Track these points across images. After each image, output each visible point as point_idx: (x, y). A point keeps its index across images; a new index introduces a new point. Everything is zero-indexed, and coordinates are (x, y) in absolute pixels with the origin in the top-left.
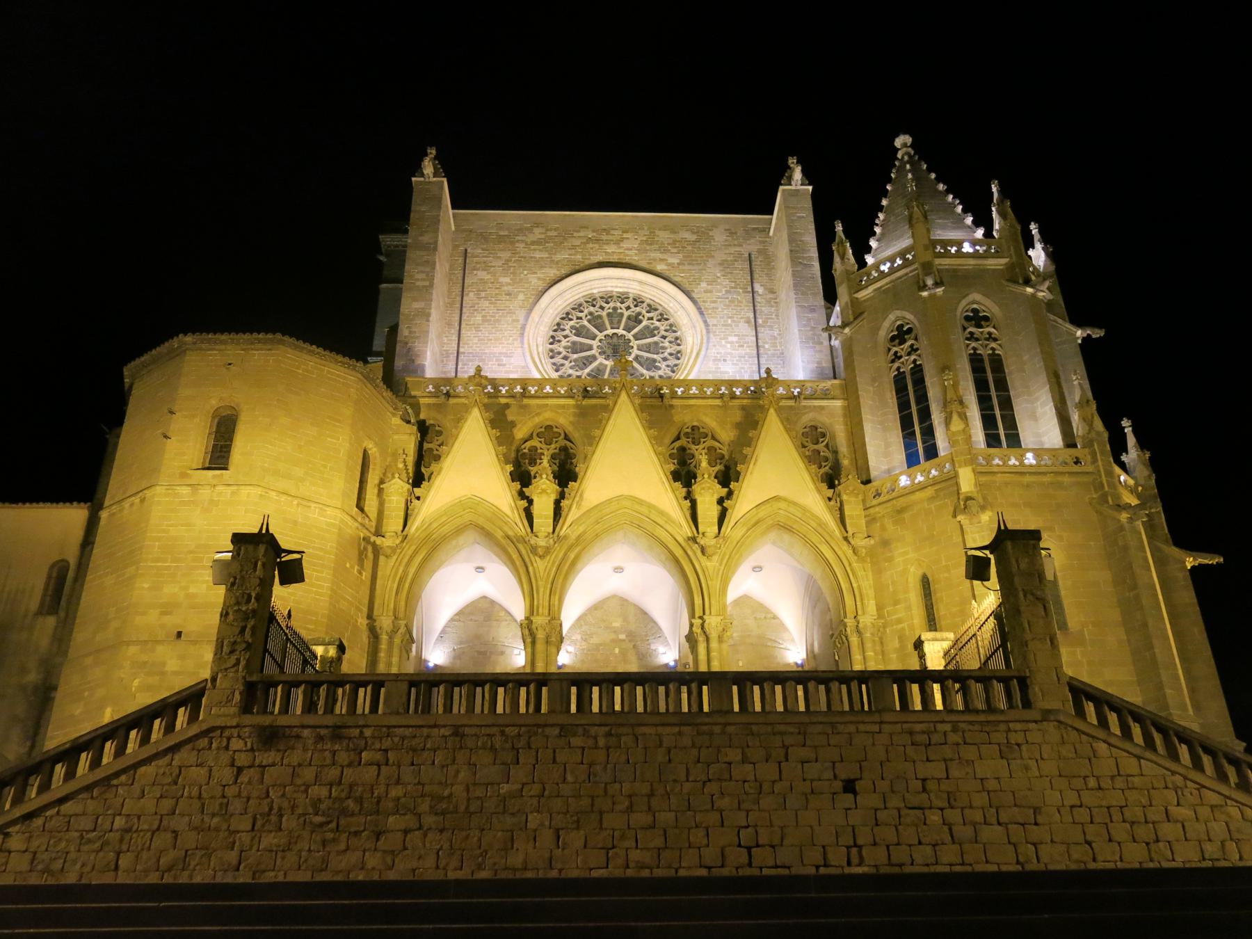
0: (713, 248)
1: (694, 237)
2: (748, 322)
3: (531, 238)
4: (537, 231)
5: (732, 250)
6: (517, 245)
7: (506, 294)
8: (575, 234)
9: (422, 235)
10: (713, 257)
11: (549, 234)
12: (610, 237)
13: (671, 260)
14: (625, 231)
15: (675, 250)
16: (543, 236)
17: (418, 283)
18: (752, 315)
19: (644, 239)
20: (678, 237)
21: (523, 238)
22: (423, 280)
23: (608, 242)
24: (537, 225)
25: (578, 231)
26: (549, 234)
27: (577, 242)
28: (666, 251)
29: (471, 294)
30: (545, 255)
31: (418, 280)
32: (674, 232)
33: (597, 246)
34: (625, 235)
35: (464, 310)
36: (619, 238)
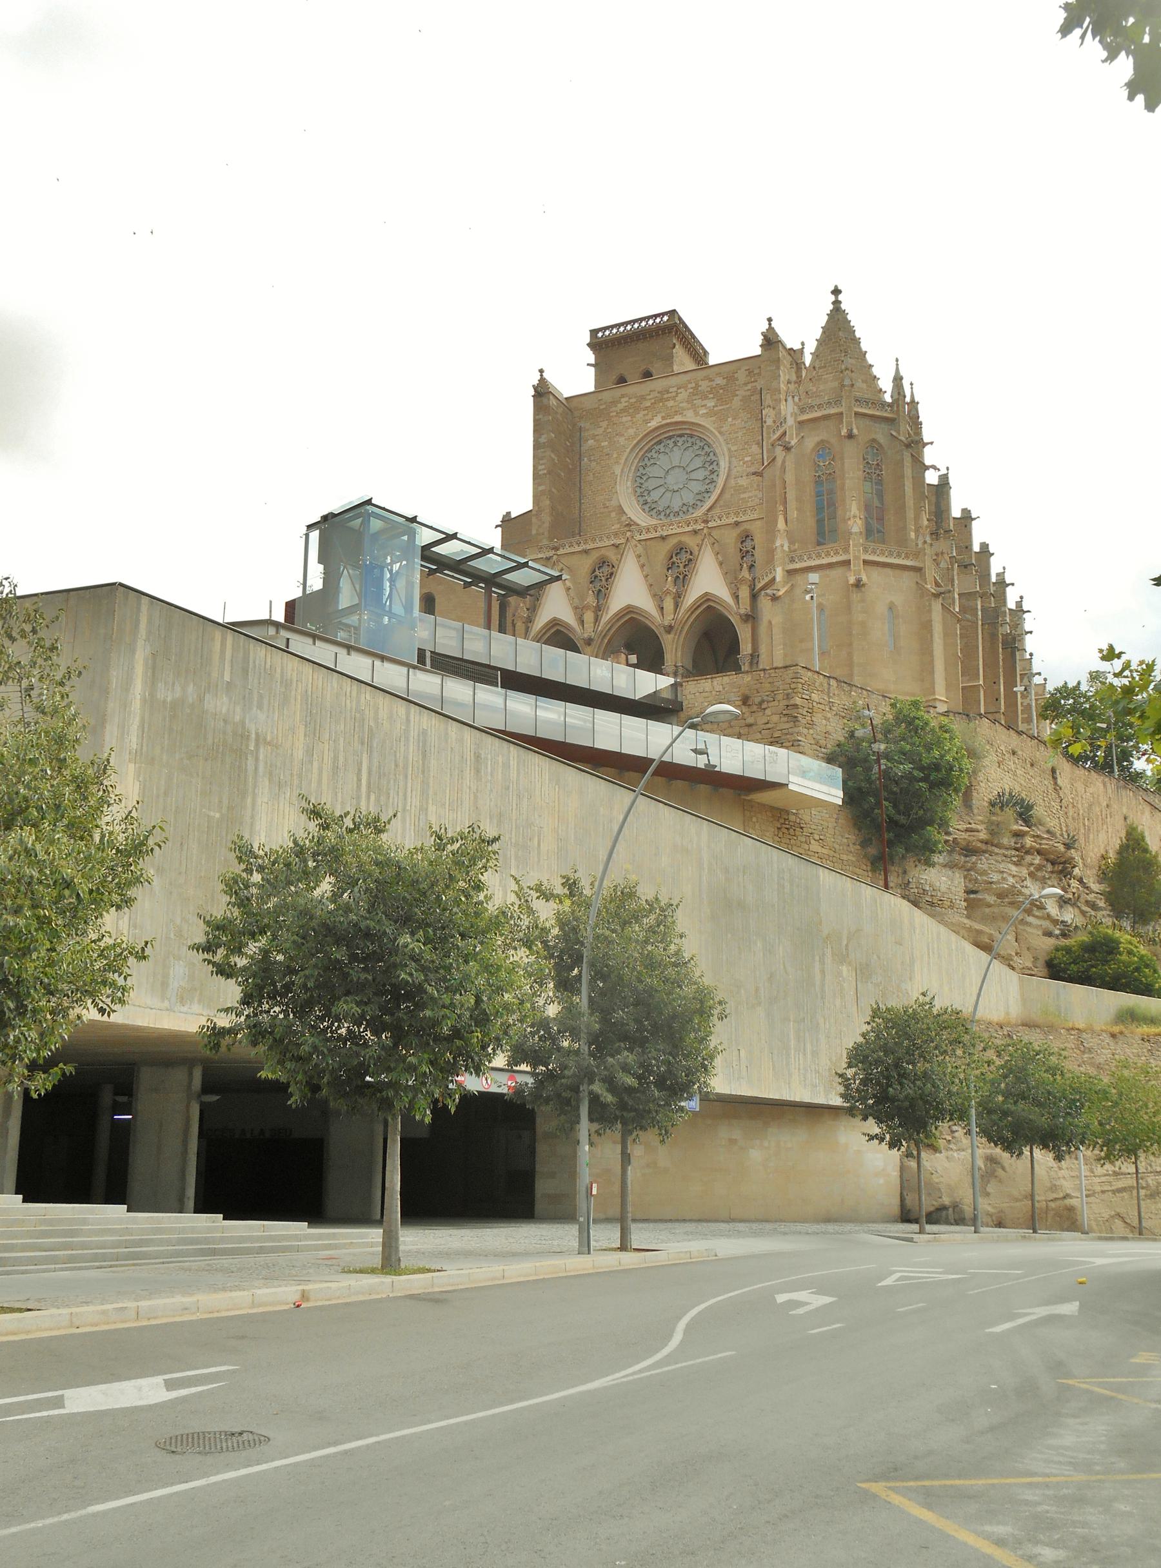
0: (737, 388)
2: (758, 444)
3: (620, 406)
5: (749, 387)
6: (611, 414)
7: (608, 454)
8: (648, 397)
9: (540, 437)
10: (737, 395)
11: (631, 401)
12: (669, 395)
13: (708, 405)
14: (680, 388)
15: (712, 396)
16: (627, 404)
17: (540, 473)
18: (761, 438)
19: (692, 390)
20: (714, 384)
21: (614, 409)
22: (543, 469)
23: (668, 400)
24: (623, 396)
25: (650, 394)
26: (631, 401)
27: (648, 404)
28: (706, 398)
29: (586, 459)
30: (629, 418)
31: (540, 470)
32: (711, 380)
33: (661, 404)
34: (679, 391)
35: (582, 472)
36: (674, 394)
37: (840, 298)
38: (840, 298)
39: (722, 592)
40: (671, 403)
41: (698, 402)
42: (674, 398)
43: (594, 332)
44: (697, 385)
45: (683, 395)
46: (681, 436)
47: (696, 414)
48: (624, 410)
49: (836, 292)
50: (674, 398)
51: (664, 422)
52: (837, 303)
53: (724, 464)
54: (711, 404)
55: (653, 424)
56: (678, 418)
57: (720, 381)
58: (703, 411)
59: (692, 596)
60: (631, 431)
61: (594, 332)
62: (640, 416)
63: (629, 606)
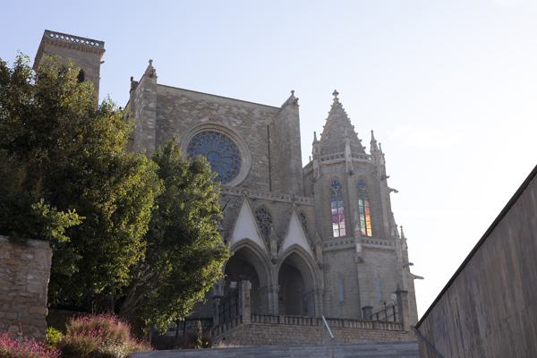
1: (246, 113)
4: (184, 99)
23: (213, 109)
24: (183, 96)
28: (236, 118)
37: (338, 97)
38: (338, 97)
39: (305, 246)
40: (214, 112)
41: (231, 118)
42: (216, 110)
43: (47, 32)
44: (230, 109)
45: (222, 111)
46: (218, 134)
47: (230, 125)
48: (184, 105)
49: (336, 93)
50: (216, 110)
51: (210, 122)
52: (336, 100)
53: (246, 161)
54: (239, 123)
55: (204, 120)
56: (219, 123)
57: (243, 111)
58: (234, 125)
59: (286, 246)
60: (190, 120)
61: (47, 32)
62: (195, 112)
63: (247, 239)
